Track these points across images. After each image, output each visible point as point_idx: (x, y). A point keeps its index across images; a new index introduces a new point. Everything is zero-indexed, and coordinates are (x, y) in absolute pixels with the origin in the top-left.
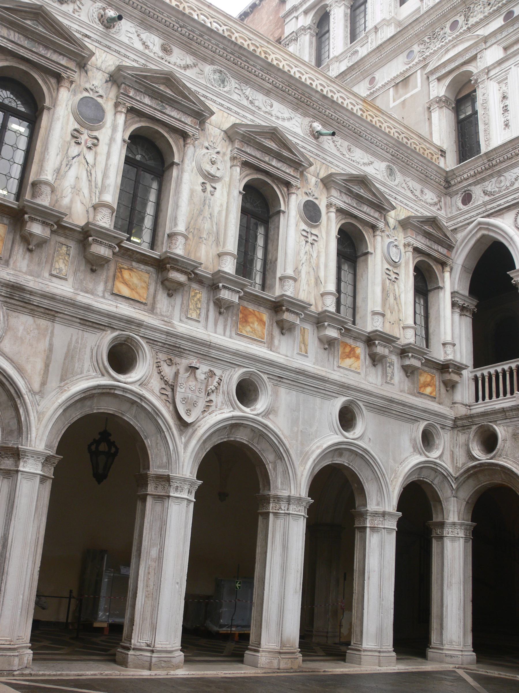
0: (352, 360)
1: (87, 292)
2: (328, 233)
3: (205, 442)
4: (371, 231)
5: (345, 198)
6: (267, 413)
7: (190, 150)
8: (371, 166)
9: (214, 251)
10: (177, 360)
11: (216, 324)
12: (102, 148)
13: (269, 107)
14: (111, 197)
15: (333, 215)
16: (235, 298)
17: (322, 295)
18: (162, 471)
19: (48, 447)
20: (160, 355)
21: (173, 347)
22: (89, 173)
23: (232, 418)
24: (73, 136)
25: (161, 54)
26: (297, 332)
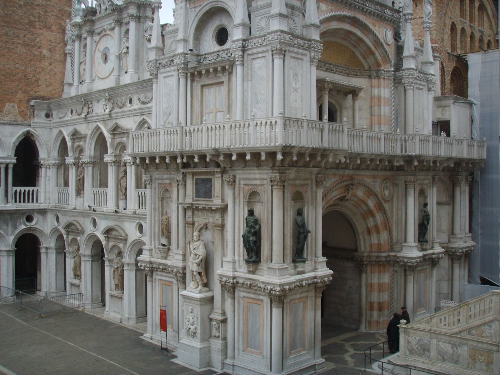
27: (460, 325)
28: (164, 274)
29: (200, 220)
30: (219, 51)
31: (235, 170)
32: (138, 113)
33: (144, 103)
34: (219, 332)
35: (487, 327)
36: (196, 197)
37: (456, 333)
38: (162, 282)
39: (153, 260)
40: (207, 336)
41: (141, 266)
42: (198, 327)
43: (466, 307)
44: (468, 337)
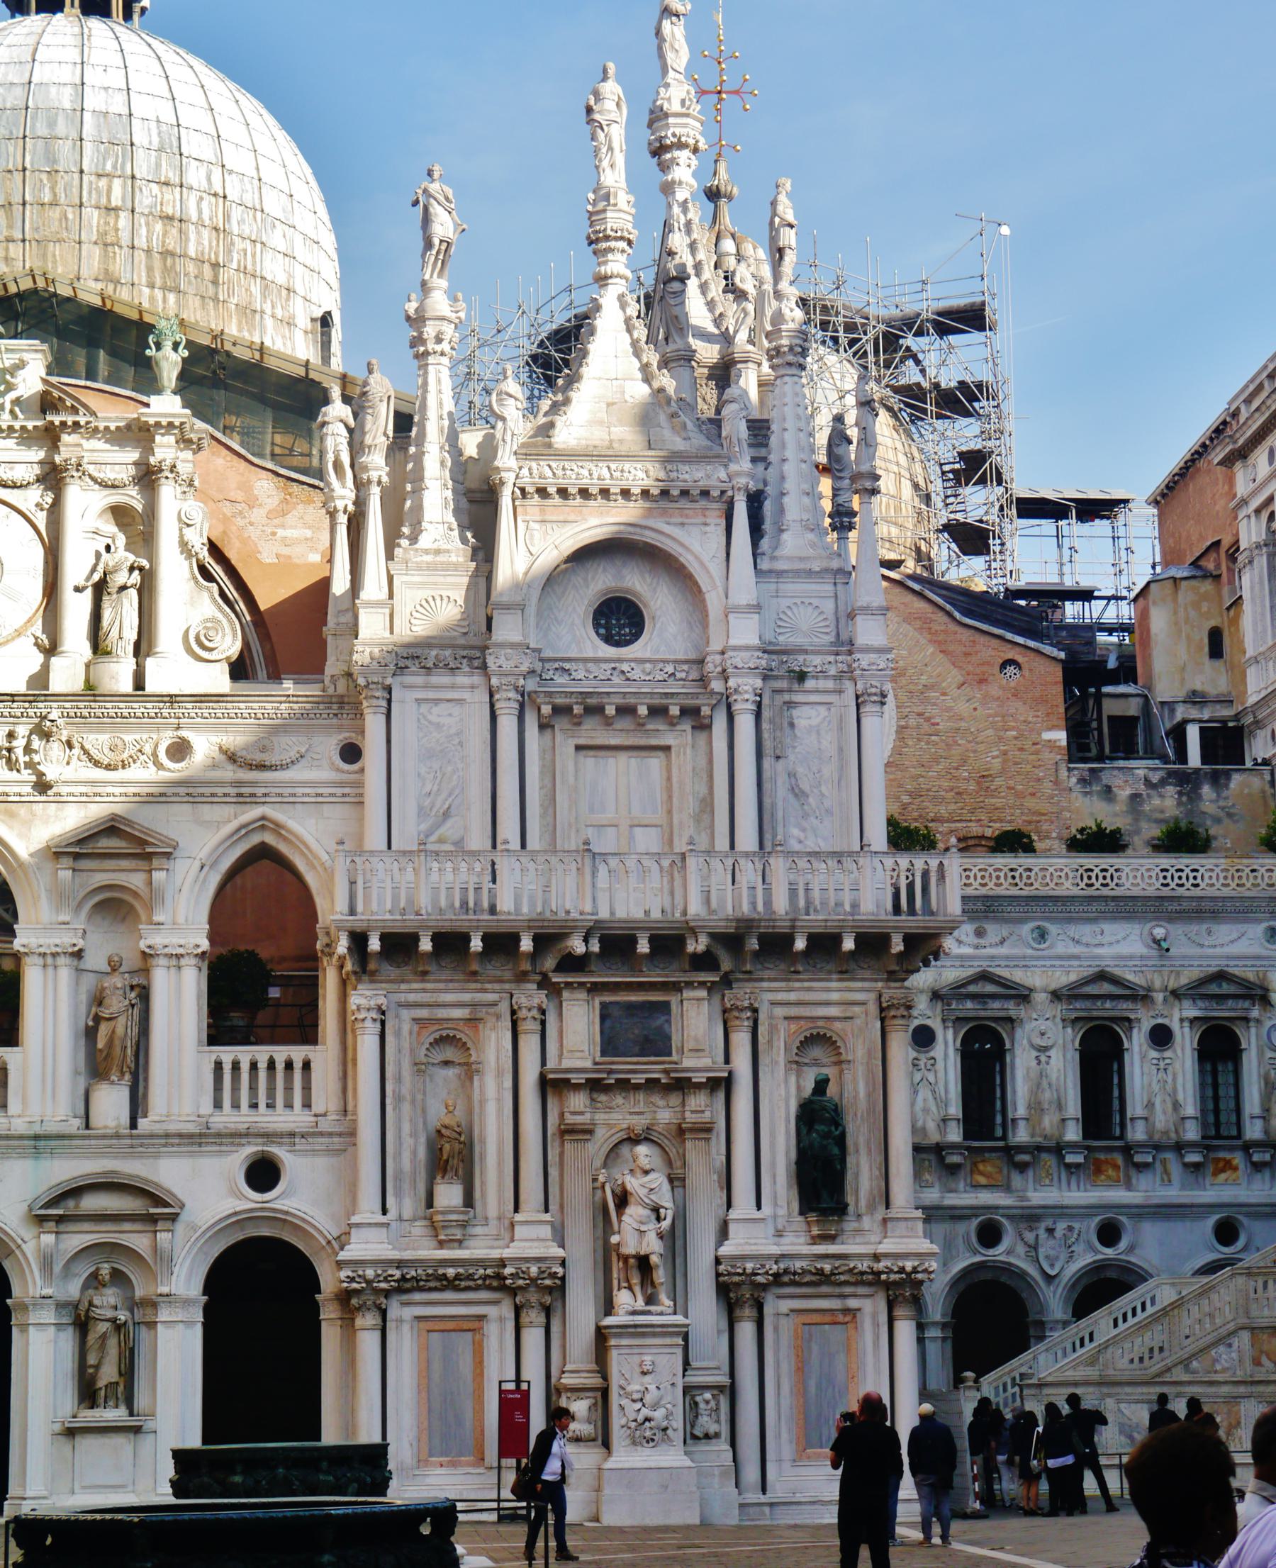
0: (1228, 1173)
1: (951, 1191)
2: (1183, 1050)
3: (1074, 1285)
4: (1243, 1023)
5: (1200, 1004)
6: (1131, 1249)
7: (1019, 1033)
8: (1244, 938)
9: (1056, 1118)
10: (1037, 1224)
11: (1069, 1184)
12: (940, 1065)
13: (1099, 937)
14: (955, 1110)
15: (1187, 1030)
16: (1079, 1159)
17: (1183, 1119)
18: (1037, 1317)
19: (943, 1315)
20: (1021, 1225)
21: (1030, 1217)
22: (934, 1091)
23: (1094, 1262)
24: (914, 1065)
25: (976, 941)
26: (1158, 1165)
27: (1166, 1353)
28: (449, 1295)
29: (621, 1114)
30: (620, 660)
31: (762, 980)
32: (225, 795)
33: (262, 767)
34: (718, 1421)
35: (1222, 1349)
36: (603, 1053)
37: (1158, 1375)
38: (430, 1325)
39: (407, 1255)
40: (693, 1437)
41: (352, 1280)
42: (670, 1409)
43: (1176, 1311)
44: (1186, 1378)
